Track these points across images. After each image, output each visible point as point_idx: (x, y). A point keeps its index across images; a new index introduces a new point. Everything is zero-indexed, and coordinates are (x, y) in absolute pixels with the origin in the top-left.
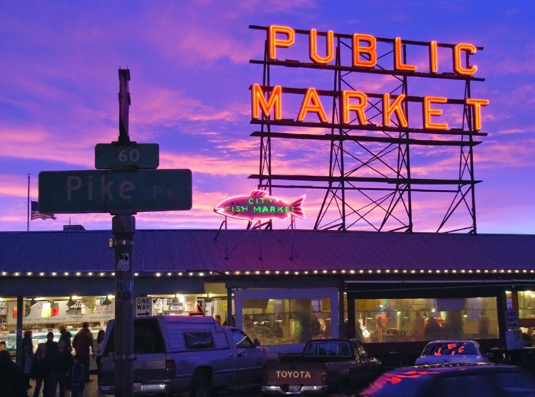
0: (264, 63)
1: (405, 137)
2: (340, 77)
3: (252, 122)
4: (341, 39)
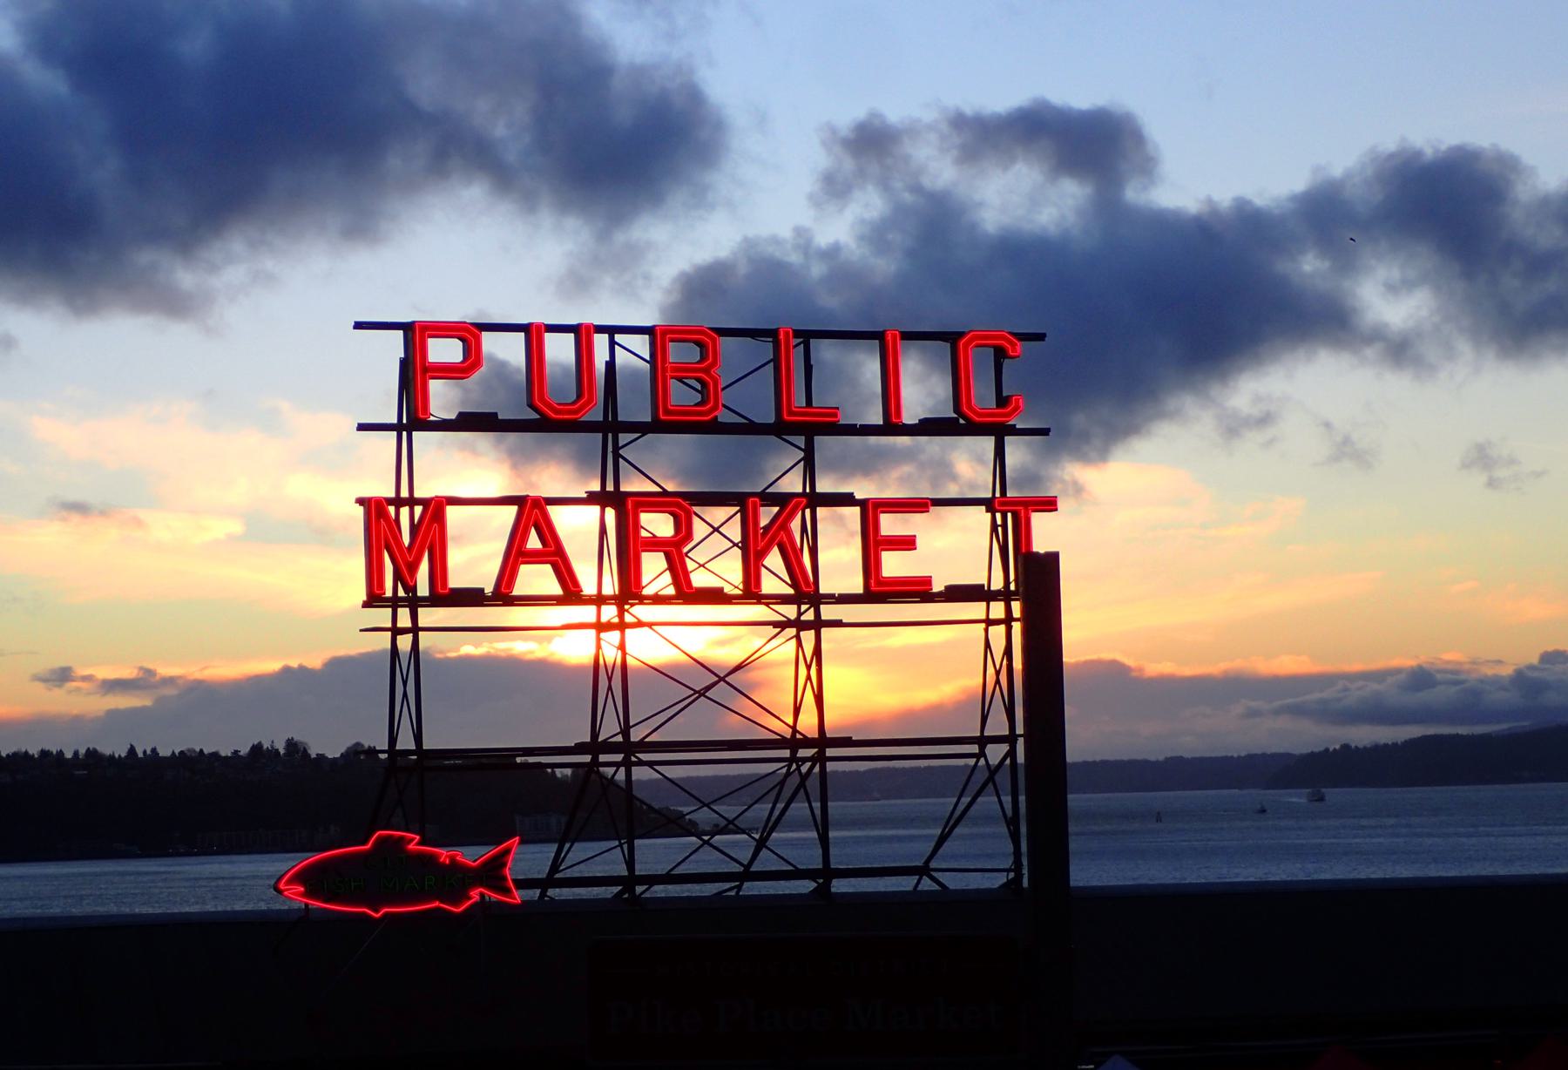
0: (397, 428)
1: (809, 616)
2: (616, 448)
3: (366, 605)
4: (618, 338)
